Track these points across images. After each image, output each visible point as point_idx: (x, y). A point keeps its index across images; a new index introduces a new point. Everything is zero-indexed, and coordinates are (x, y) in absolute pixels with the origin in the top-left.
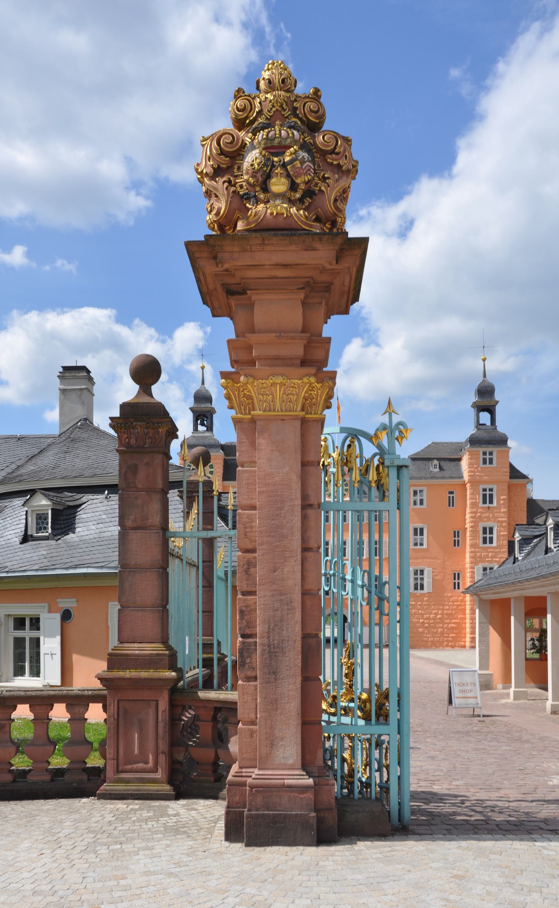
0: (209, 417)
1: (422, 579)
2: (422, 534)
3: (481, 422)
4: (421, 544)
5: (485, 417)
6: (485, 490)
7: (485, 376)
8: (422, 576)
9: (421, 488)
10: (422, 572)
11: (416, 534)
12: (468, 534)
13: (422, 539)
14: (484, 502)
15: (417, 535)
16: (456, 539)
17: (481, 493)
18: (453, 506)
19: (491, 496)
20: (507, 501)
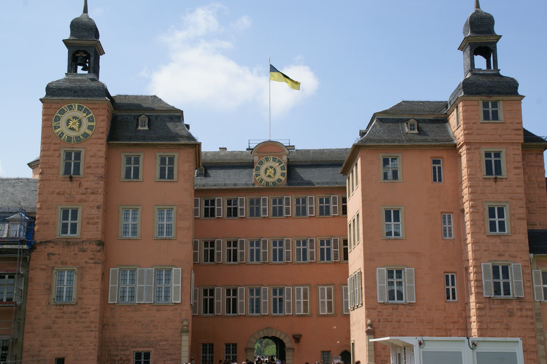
0: (92, 54)
1: (400, 284)
2: (397, 219)
3: (475, 68)
4: (397, 234)
5: (480, 62)
6: (488, 155)
7: (478, 6)
8: (399, 280)
9: (394, 155)
10: (399, 273)
11: (388, 219)
12: (467, 217)
13: (397, 227)
14: (489, 172)
15: (390, 221)
16: (447, 226)
17: (484, 159)
18: (440, 180)
19: (498, 163)
20: (521, 171)
